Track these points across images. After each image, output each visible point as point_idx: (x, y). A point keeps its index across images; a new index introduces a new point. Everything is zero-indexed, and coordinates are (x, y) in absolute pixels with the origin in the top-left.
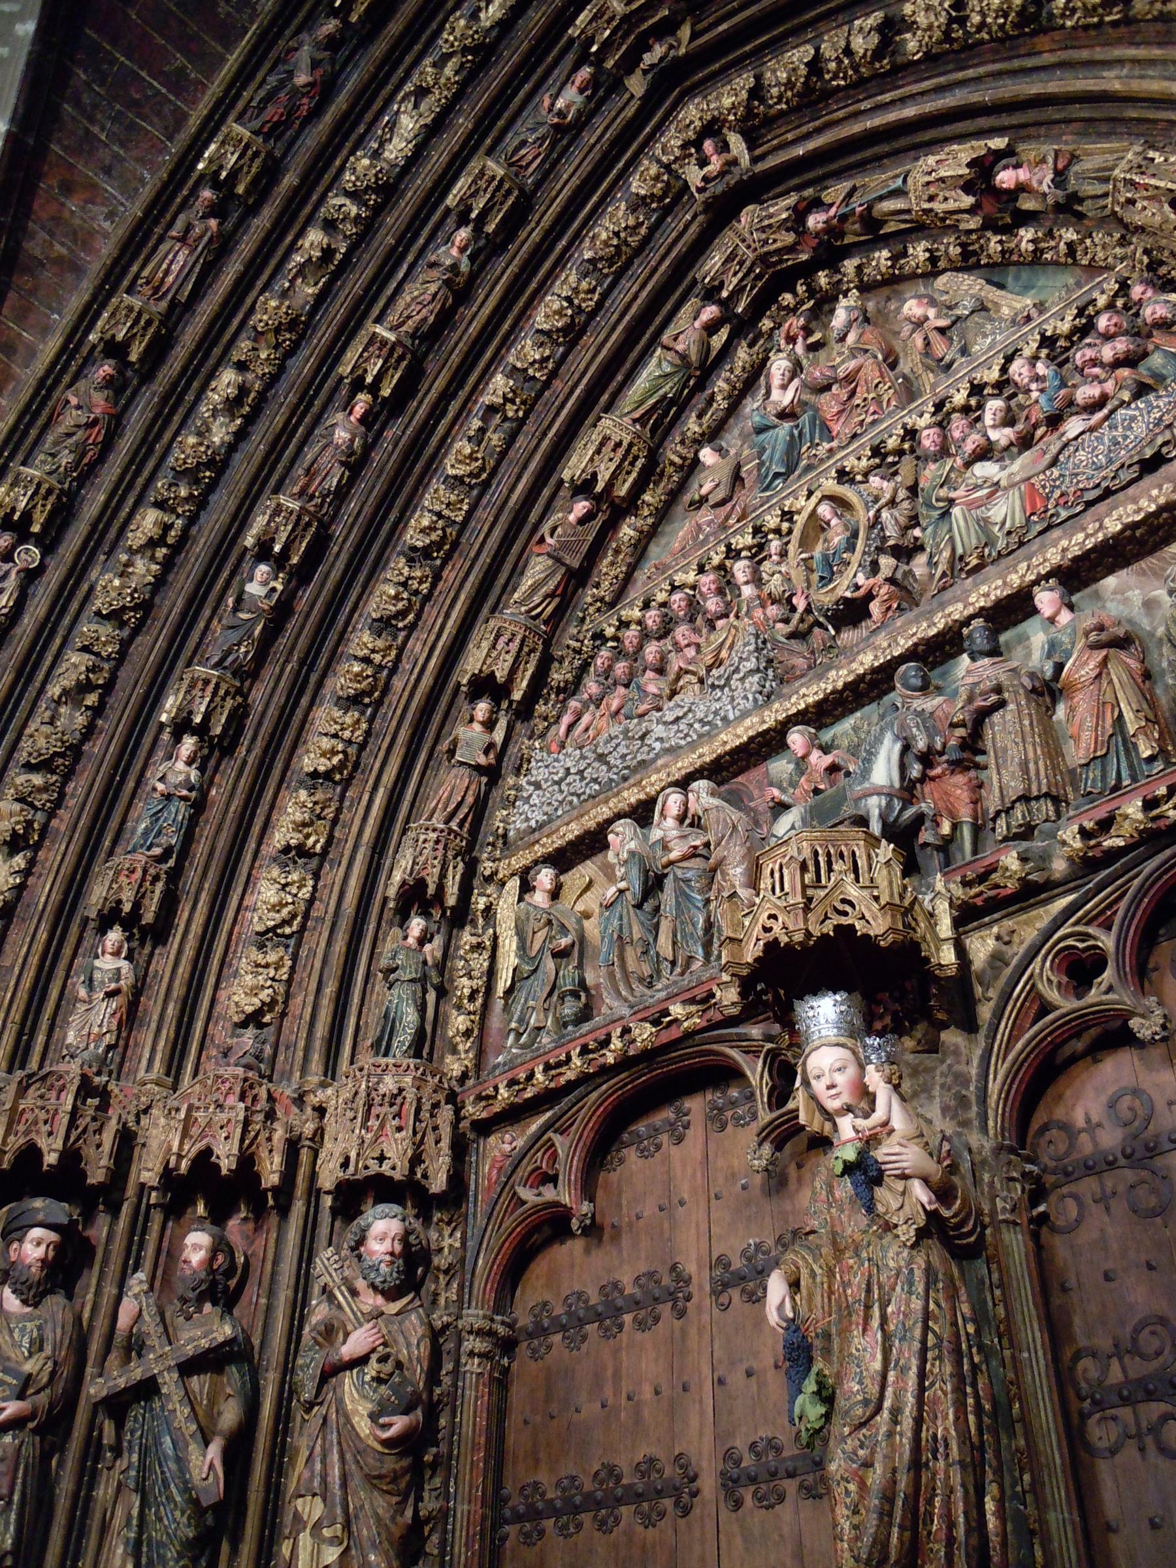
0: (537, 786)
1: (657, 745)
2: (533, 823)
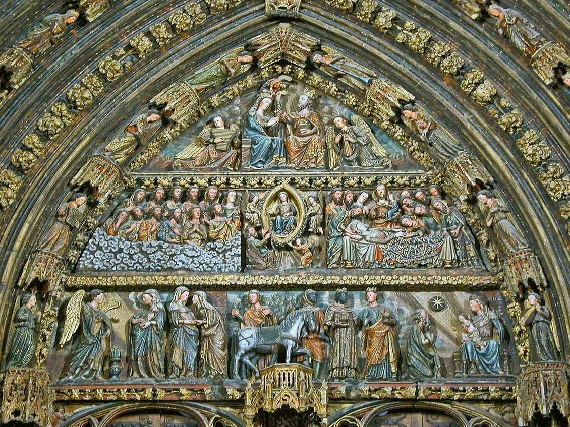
1: (180, 263)
2: (96, 267)
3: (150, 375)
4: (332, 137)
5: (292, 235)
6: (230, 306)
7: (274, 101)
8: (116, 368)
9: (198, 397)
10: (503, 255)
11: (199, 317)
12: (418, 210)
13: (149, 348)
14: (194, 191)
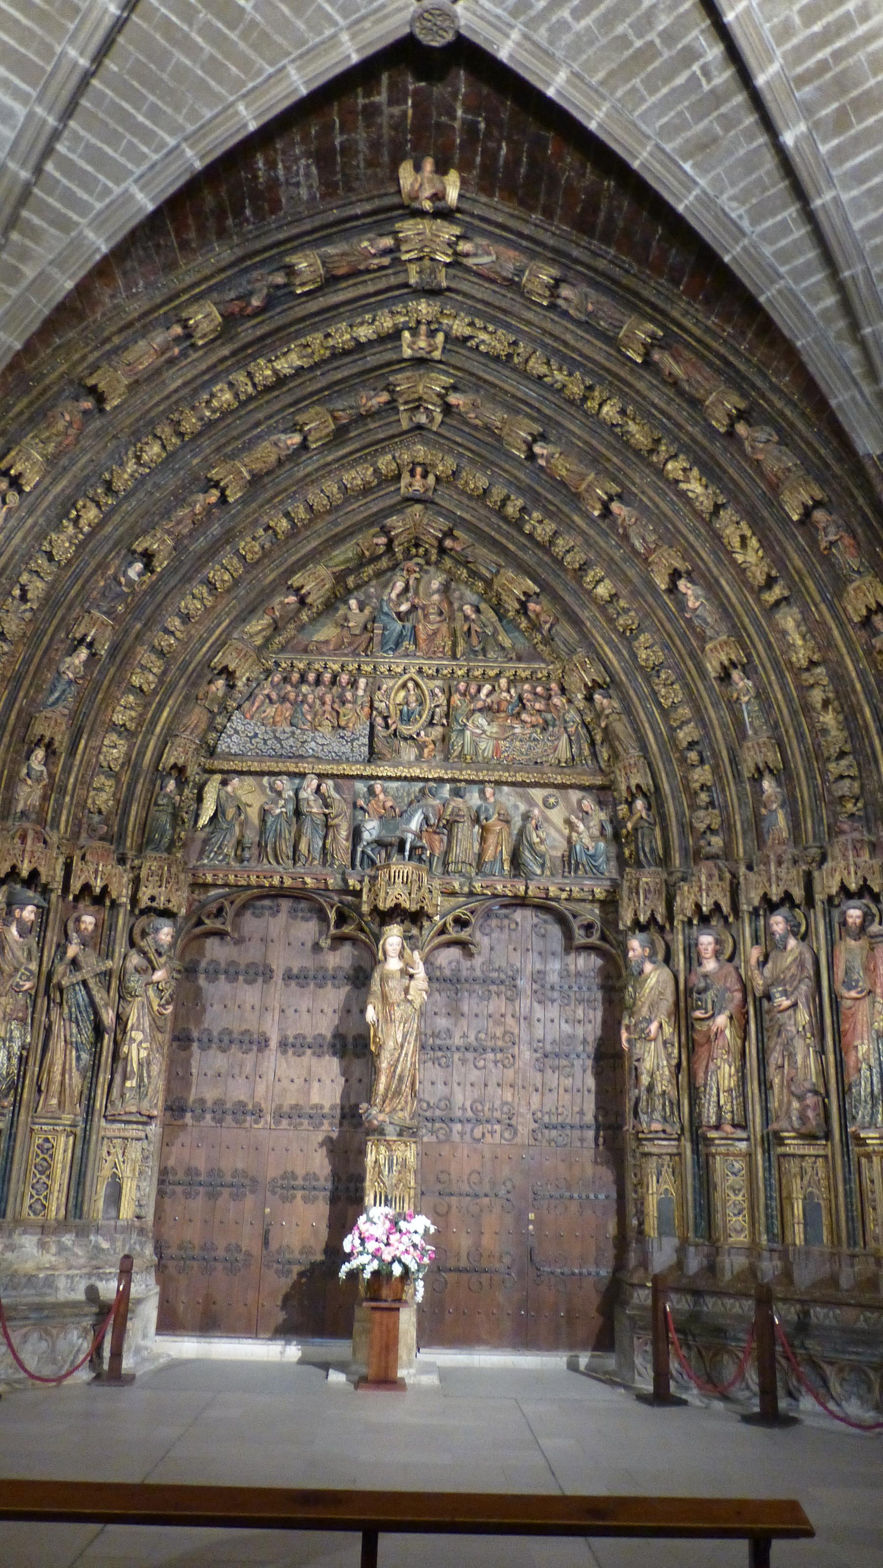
0: (237, 732)
3: (278, 863)
4: (461, 626)
5: (418, 726)
6: (356, 795)
7: (407, 584)
8: (247, 855)
9: (322, 886)
10: (615, 755)
11: (327, 806)
12: (537, 706)
13: (279, 835)
14: (327, 677)
